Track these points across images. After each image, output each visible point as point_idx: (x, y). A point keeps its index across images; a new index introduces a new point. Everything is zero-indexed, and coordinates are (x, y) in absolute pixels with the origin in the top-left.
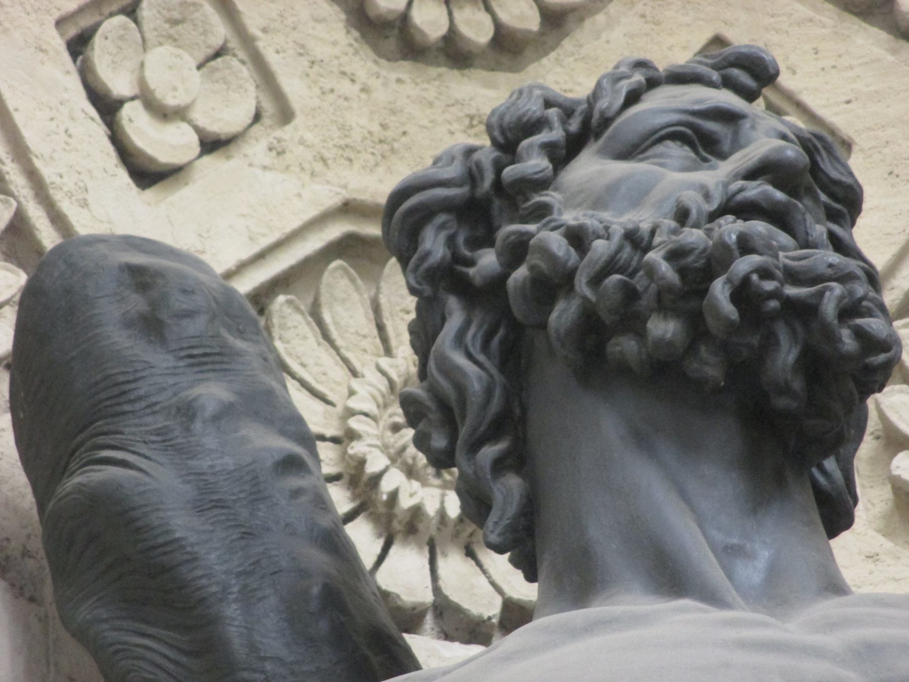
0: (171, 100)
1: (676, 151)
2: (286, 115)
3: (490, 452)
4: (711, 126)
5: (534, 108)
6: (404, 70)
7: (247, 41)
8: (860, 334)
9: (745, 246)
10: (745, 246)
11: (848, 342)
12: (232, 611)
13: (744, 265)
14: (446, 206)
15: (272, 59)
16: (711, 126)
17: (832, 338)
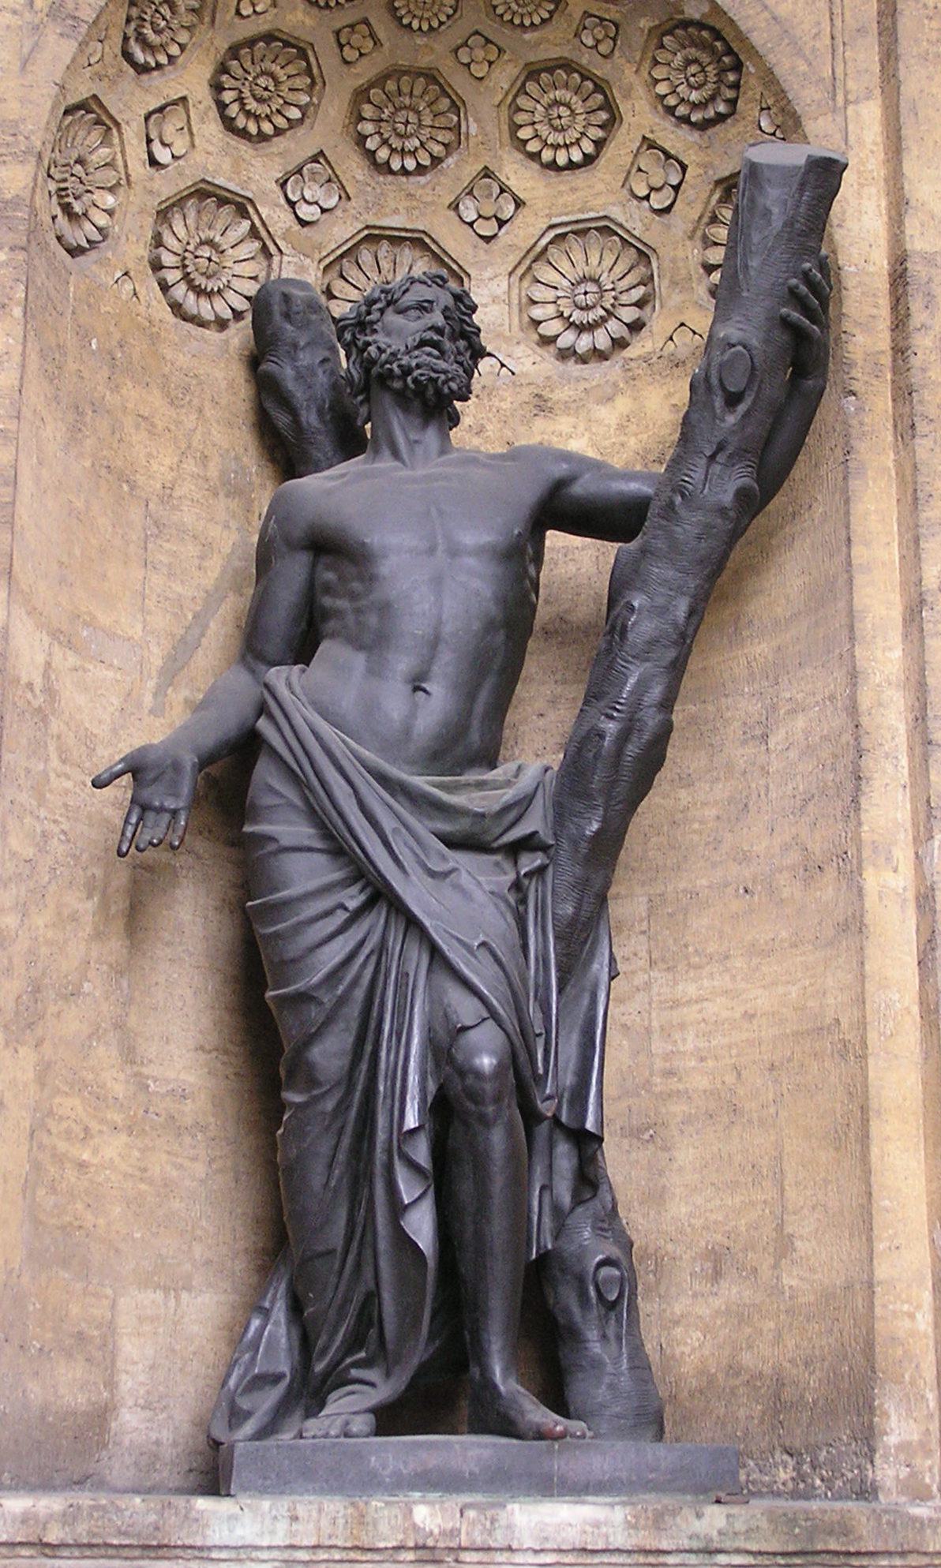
0: (311, 200)
1: (413, 313)
2: (349, 198)
3: (360, 398)
4: (426, 304)
5: (376, 295)
6: (390, 178)
7: (337, 176)
8: (449, 388)
9: (418, 366)
10: (418, 366)
11: (446, 390)
12: (303, 413)
13: (416, 373)
14: (352, 325)
15: (344, 182)
16: (426, 304)
17: (442, 390)
